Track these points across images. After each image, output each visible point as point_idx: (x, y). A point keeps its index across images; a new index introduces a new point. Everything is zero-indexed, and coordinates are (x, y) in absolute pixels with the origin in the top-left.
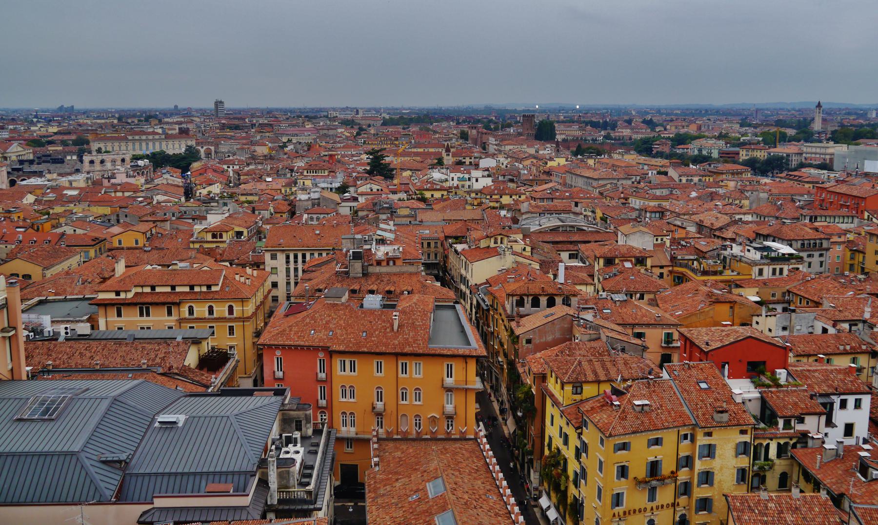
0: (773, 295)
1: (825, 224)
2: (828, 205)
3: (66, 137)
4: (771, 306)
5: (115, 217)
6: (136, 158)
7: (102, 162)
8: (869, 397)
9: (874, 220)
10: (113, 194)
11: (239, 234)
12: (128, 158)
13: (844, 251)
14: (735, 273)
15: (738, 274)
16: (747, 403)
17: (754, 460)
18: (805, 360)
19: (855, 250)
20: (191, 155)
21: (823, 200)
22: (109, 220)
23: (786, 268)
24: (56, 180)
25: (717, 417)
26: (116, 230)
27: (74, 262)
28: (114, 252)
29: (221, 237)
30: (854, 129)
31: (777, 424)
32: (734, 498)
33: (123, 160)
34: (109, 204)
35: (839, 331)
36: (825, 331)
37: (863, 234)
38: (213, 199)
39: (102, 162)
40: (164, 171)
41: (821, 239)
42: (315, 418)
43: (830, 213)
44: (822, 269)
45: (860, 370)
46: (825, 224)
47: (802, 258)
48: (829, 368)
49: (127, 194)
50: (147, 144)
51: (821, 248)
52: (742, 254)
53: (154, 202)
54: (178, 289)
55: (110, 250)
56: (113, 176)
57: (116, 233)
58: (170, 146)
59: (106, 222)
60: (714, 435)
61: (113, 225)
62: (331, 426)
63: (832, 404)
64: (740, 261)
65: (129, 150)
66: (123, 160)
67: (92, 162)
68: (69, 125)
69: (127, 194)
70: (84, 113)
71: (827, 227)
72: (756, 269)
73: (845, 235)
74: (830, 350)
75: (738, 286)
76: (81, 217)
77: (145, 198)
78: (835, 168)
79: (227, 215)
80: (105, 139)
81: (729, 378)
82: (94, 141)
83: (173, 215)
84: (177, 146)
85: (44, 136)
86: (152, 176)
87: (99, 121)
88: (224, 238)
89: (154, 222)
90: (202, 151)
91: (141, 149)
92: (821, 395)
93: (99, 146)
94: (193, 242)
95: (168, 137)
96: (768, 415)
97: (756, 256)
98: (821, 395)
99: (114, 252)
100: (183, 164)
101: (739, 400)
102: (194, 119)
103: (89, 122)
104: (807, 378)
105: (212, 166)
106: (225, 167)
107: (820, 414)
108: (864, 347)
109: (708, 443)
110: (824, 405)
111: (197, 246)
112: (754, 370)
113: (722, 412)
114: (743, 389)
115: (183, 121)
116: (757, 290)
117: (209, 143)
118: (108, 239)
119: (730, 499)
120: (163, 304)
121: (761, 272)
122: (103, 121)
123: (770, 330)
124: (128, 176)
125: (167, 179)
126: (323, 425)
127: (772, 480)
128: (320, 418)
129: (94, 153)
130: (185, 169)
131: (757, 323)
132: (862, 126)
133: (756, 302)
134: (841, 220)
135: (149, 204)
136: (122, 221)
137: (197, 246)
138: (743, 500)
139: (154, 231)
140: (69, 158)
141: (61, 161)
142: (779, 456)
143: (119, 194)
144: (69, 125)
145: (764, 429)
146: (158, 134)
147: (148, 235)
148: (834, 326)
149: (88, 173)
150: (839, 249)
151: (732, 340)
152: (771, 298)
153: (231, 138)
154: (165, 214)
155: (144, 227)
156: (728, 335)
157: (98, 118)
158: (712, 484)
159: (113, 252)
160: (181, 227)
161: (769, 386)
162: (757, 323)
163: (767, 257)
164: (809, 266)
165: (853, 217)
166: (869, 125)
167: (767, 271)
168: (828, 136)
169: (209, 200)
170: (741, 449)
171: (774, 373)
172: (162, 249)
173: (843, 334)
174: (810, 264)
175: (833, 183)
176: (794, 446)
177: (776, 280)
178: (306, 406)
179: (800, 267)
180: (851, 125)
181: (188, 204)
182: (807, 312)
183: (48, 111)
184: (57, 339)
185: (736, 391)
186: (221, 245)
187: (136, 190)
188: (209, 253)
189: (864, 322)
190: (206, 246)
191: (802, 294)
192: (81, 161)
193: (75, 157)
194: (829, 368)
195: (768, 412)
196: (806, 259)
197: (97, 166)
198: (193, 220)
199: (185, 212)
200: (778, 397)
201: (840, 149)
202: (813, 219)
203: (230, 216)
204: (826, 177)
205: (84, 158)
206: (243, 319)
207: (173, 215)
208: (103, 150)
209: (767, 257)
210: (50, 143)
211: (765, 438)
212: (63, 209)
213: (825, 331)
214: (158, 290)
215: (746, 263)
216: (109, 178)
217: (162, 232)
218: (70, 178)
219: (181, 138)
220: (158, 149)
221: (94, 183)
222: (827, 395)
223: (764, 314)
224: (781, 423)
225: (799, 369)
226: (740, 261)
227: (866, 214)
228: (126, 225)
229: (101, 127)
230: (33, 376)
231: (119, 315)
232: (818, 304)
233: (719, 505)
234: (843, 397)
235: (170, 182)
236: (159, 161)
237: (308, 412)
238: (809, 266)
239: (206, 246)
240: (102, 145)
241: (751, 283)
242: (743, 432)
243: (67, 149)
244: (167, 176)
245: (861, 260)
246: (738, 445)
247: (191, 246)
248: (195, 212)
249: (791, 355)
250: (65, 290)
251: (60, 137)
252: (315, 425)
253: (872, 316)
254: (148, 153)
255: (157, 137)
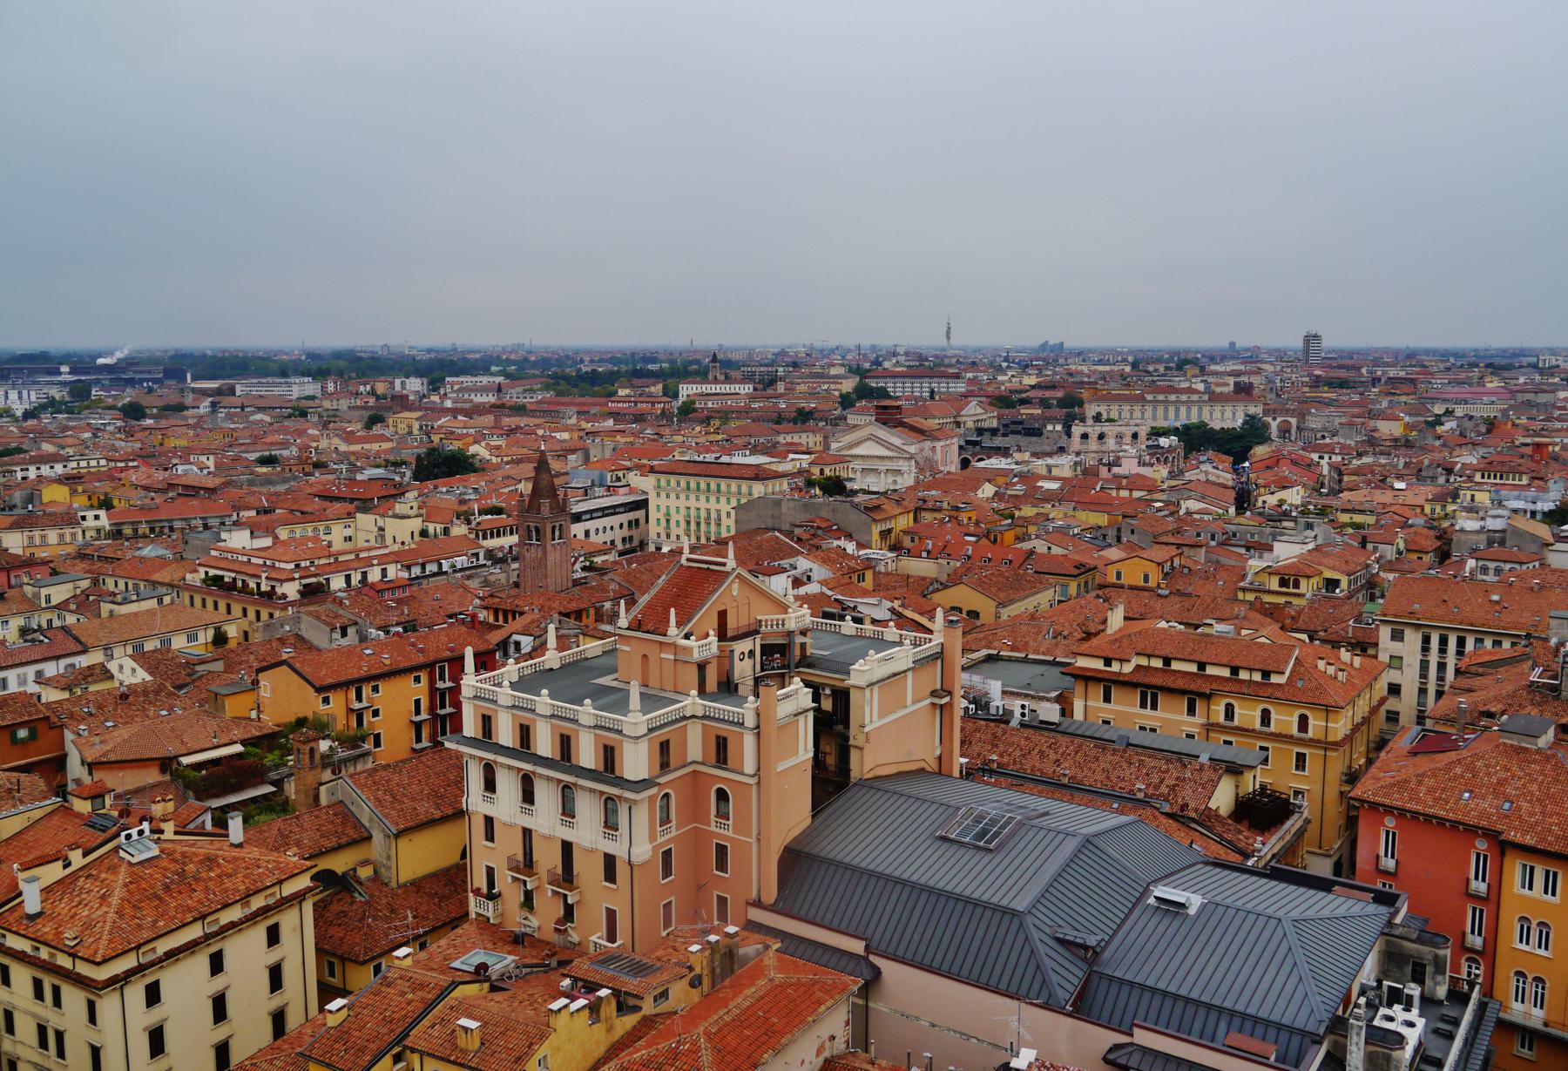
3: (1048, 394)
5: (1115, 533)
6: (1156, 433)
7: (1101, 437)
10: (1114, 493)
11: (1332, 584)
12: (1143, 432)
20: (1254, 432)
22: (1104, 536)
24: (1027, 462)
26: (1114, 553)
27: (1043, 599)
28: (1108, 591)
29: (1297, 585)
33: (1135, 436)
34: (1108, 508)
38: (1286, 515)
39: (1101, 437)
40: (1203, 458)
42: (1456, 968)
49: (1137, 494)
50: (1177, 410)
53: (1182, 512)
54: (1210, 670)
55: (1101, 587)
56: (1117, 463)
57: (1115, 558)
58: (1217, 414)
59: (1100, 537)
61: (1110, 546)
62: (1488, 992)
65: (1145, 418)
66: (1135, 436)
67: (1085, 436)
68: (1055, 373)
69: (1137, 494)
70: (1079, 354)
76: (1061, 527)
77: (1167, 503)
79: (1311, 546)
80: (1109, 398)
82: (1091, 402)
83: (1213, 538)
84: (1229, 414)
85: (1016, 392)
86: (1182, 465)
87: (1101, 368)
88: (1303, 589)
89: (1179, 546)
90: (1274, 425)
91: (1166, 418)
93: (1098, 409)
94: (1244, 590)
95: (1214, 398)
99: (1108, 591)
100: (1237, 446)
102: (1263, 366)
103: (1085, 369)
105: (1290, 453)
106: (1315, 457)
111: (1250, 597)
115: (1244, 373)
117: (1288, 412)
118: (1101, 567)
120: (1182, 692)
122: (1107, 368)
124: (1141, 463)
125: (1206, 473)
126: (1472, 985)
128: (1465, 969)
129: (1090, 422)
130: (1240, 455)
135: (1172, 514)
136: (1124, 539)
137: (1250, 597)
139: (1176, 562)
140: (1050, 427)
141: (1038, 433)
143: (1124, 493)
144: (1055, 373)
146: (1196, 392)
147: (1167, 568)
149: (1078, 454)
153: (1330, 403)
154: (1198, 535)
155: (1160, 553)
157: (1100, 362)
159: (1107, 590)
160: (1223, 560)
169: (1280, 515)
172: (1189, 595)
178: (1440, 940)
181: (1241, 520)
183: (1024, 350)
184: (1007, 722)
186: (1295, 601)
187: (1152, 488)
188: (1273, 612)
190: (1267, 598)
192: (1069, 434)
193: (1059, 427)
197: (1093, 445)
198: (1248, 549)
199: (1234, 535)
203: (1317, 549)
205: (1074, 429)
206: (1326, 745)
207: (1213, 538)
208: (1105, 416)
210: (1024, 402)
212: (1035, 510)
214: (1175, 666)
216: (1110, 465)
217: (1189, 563)
218: (1050, 461)
219: (1238, 400)
220: (1194, 420)
221: (1085, 472)
228: (1131, 547)
229: (1104, 378)
230: (969, 774)
231: (1107, 699)
235: (1211, 478)
236: (1196, 439)
237: (1441, 952)
239: (1267, 598)
240: (1102, 409)
243: (1048, 413)
244: (1207, 467)
247: (1240, 596)
248: (1253, 535)
250: (1027, 644)
251: (1039, 393)
252: (1454, 981)
254: (1178, 424)
255: (1195, 397)
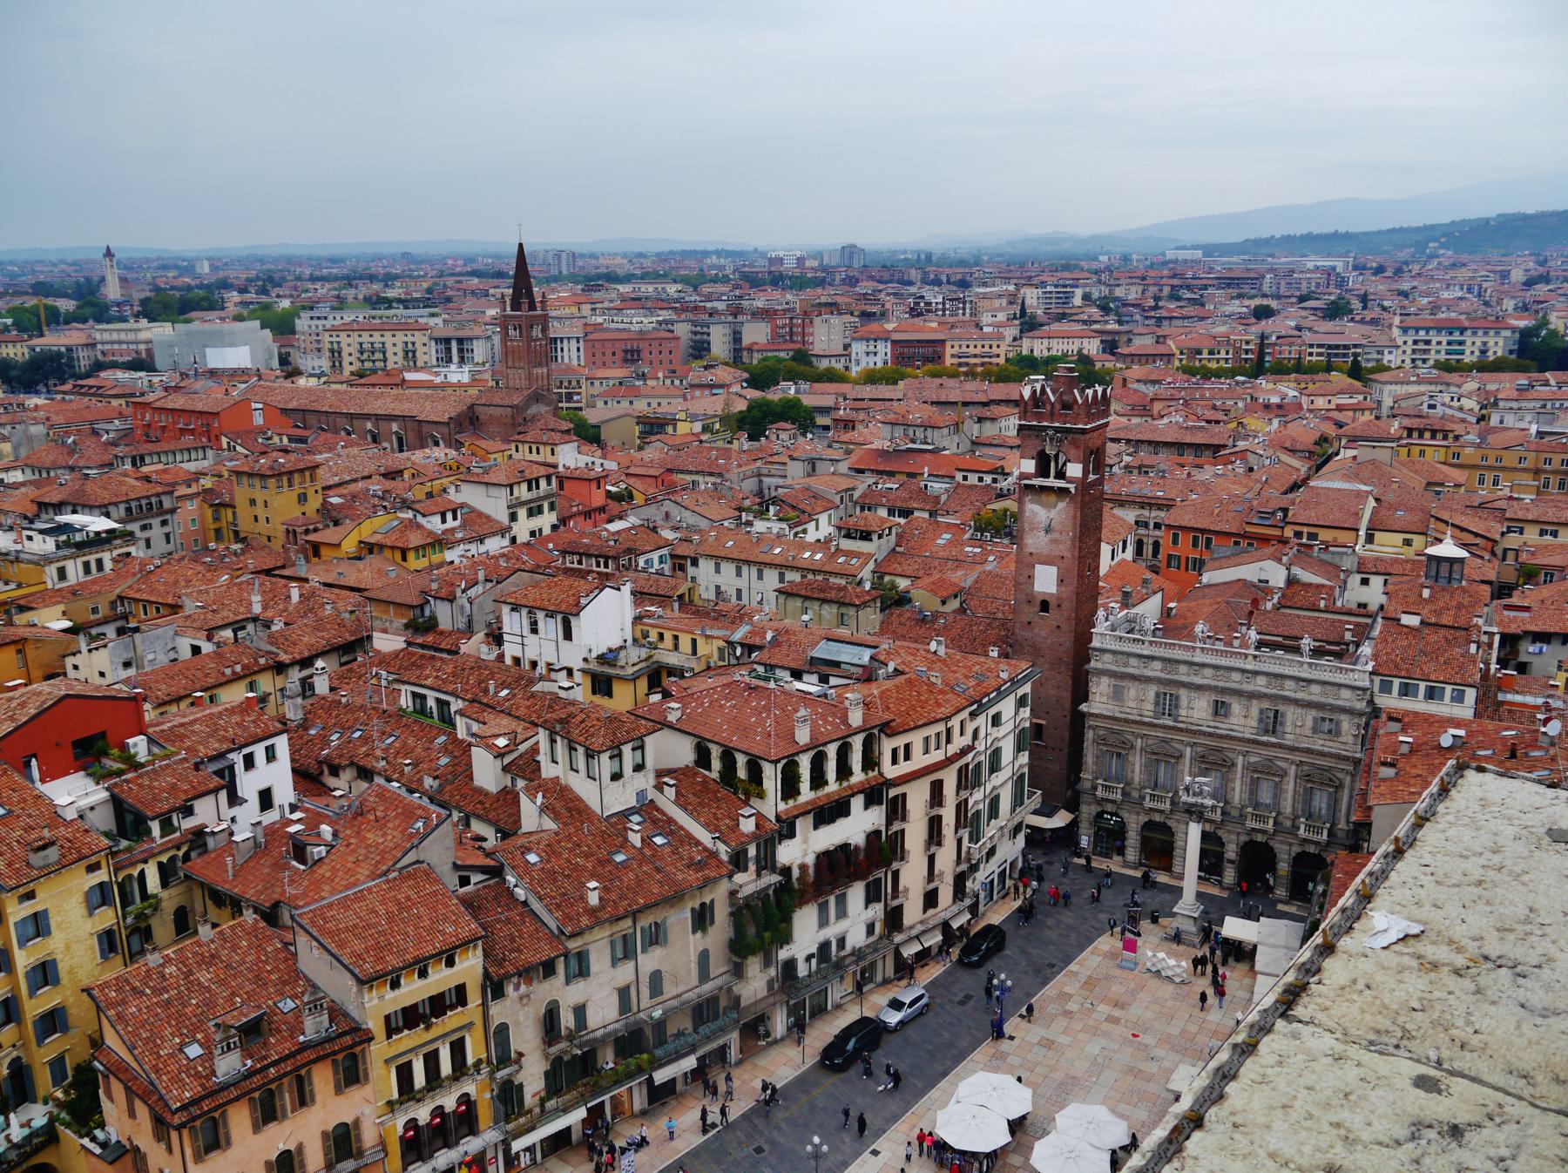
0: (95, 610)
1: (160, 467)
2: (158, 433)
4: (94, 631)
8: (284, 737)
9: (238, 448)
13: (201, 508)
14: (13, 586)
15: (19, 586)
16: (90, 815)
17: (123, 907)
18: (173, 709)
19: (218, 503)
21: (149, 426)
23: (107, 557)
25: (37, 859)
30: (178, 294)
31: (149, 831)
32: (102, 987)
35: (218, 645)
36: (196, 650)
37: (226, 474)
41: (158, 495)
43: (164, 446)
44: (171, 547)
45: (263, 699)
46: (160, 467)
47: (131, 534)
48: (215, 710)
51: (161, 511)
52: (19, 547)
60: (40, 895)
63: (231, 768)
64: (18, 560)
71: (165, 471)
72: (51, 571)
73: (197, 480)
74: (211, 681)
75: (23, 609)
78: (158, 366)
81: (43, 781)
92: (212, 759)
96: (129, 820)
97: (47, 545)
98: (212, 759)
101: (71, 814)
104: (182, 737)
107: (216, 791)
108: (262, 661)
109: (31, 911)
110: (220, 773)
112: (88, 752)
113: (44, 847)
114: (75, 794)
116: (61, 607)
119: (96, 992)
121: (62, 574)
123: (102, 674)
127: (162, 928)
131: (76, 667)
132: (189, 288)
133: (65, 631)
134: (186, 457)
138: (120, 983)
142: (165, 884)
145: (128, 850)
148: (209, 638)
150: (191, 506)
151: (33, 711)
152: (92, 617)
156: (23, 705)
158: (56, 981)
161: (120, 773)
162: (76, 667)
163: (67, 544)
164: (148, 546)
165: (204, 448)
166: (200, 287)
167: (74, 570)
168: (136, 309)
170: (97, 898)
171: (124, 748)
173: (226, 649)
174: (148, 541)
175: (160, 393)
176: (187, 857)
177: (94, 582)
179: (132, 550)
180: (172, 288)
182: (159, 626)
185: (61, 800)
189: (255, 619)
191: (144, 597)
194: (215, 710)
195: (129, 818)
196: (138, 534)
200: (140, 786)
201: (160, 332)
202: (137, 461)
204: (146, 383)
209: (67, 544)
211: (133, 864)
213: (196, 650)
215: (30, 562)
222: (221, 755)
223: (84, 647)
224: (155, 827)
225: (165, 727)
226: (18, 560)
227: (224, 440)
232: (175, 608)
233: (80, 1011)
234: (246, 751)
238: (148, 546)
241: (48, 597)
242: (92, 868)
245: (230, 519)
246: (88, 895)
249: (147, 706)
253: (265, 608)
